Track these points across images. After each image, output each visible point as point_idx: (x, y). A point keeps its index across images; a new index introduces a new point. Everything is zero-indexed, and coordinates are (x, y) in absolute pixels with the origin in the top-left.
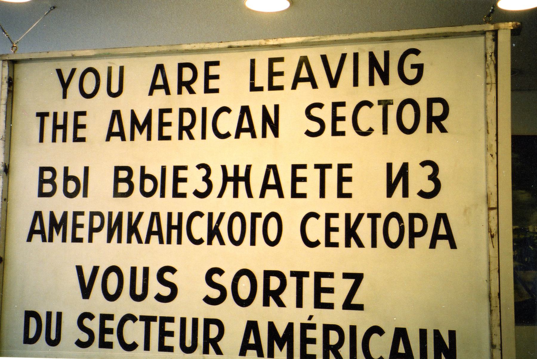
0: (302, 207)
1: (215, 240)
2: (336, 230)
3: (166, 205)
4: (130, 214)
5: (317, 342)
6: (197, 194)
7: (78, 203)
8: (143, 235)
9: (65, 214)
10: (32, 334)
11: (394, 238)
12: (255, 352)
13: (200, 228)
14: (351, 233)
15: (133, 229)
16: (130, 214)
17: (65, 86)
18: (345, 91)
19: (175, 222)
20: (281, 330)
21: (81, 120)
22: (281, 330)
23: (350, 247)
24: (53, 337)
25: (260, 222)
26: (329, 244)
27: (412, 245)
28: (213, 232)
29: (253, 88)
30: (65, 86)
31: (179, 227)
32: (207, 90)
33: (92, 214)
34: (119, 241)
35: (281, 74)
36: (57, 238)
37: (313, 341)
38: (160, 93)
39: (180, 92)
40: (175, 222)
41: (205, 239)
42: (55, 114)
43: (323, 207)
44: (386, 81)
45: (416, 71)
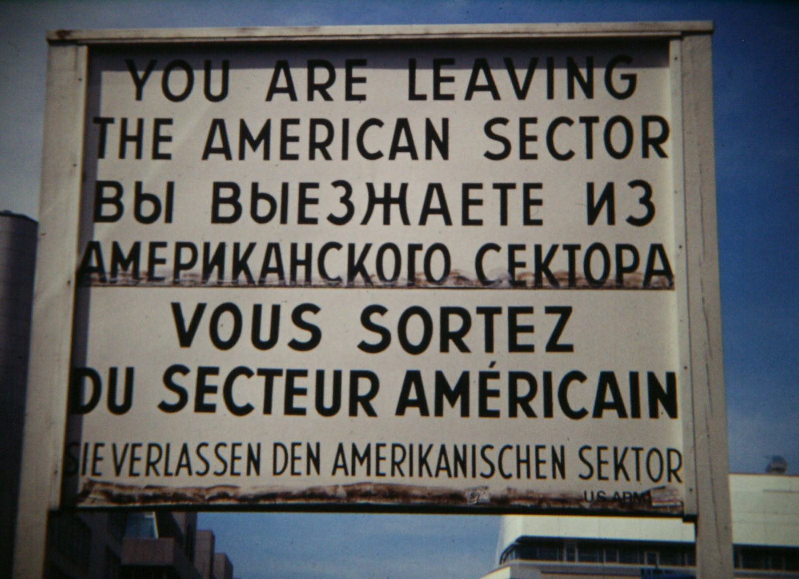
3: (288, 234)
4: (237, 246)
6: (332, 219)
7: (158, 230)
9: (136, 247)
15: (240, 265)
16: (237, 246)
20: (453, 384)
21: (164, 130)
22: (453, 384)
25: (420, 256)
28: (355, 268)
29: (413, 96)
32: (350, 97)
33: (179, 246)
37: (496, 394)
38: (281, 98)
39: (311, 97)
42: (124, 122)
43: (505, 237)
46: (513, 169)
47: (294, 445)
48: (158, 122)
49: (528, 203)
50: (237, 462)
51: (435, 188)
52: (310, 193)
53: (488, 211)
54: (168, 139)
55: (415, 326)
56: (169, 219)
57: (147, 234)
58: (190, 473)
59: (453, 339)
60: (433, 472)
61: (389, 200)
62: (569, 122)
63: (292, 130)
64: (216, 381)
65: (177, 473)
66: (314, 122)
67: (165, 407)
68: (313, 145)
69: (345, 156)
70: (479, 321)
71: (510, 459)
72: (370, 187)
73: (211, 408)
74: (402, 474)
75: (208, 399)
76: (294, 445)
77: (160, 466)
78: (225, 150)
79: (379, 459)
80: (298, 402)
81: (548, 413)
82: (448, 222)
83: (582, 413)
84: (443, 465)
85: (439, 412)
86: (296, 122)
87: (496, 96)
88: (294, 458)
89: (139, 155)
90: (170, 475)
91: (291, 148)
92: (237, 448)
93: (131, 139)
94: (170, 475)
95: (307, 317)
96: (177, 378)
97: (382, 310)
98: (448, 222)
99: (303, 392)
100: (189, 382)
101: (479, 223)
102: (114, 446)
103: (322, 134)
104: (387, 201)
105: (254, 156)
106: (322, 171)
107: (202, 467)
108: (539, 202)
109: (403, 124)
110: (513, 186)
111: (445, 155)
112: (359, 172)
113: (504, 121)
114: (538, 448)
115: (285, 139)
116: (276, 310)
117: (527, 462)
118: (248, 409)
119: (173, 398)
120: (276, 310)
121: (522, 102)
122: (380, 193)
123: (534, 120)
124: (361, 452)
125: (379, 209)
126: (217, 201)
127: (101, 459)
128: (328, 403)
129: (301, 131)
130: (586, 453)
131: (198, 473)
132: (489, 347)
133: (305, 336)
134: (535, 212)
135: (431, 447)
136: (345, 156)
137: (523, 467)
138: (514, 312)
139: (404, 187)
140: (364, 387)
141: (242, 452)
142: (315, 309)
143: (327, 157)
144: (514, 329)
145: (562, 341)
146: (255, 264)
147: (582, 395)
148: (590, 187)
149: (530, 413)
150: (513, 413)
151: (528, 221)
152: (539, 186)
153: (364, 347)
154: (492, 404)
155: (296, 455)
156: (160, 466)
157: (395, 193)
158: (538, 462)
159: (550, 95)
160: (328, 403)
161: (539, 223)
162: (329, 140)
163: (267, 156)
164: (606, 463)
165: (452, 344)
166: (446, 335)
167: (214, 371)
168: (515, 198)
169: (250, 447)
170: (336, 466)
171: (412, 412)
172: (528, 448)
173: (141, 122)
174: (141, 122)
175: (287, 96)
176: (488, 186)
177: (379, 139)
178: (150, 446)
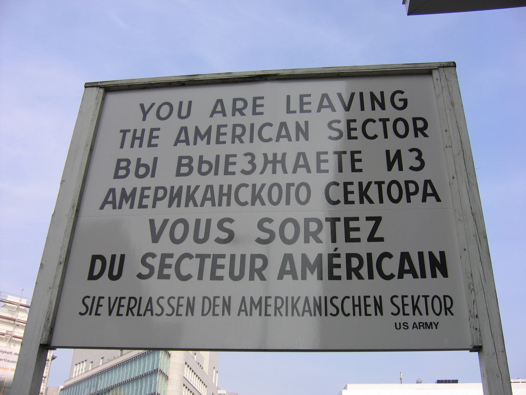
1: (258, 202)
2: (352, 192)
3: (217, 180)
4: (189, 187)
7: (147, 181)
9: (135, 190)
10: (96, 272)
11: (395, 196)
13: (245, 195)
14: (363, 194)
15: (190, 197)
16: (189, 187)
17: (145, 114)
19: (225, 191)
21: (155, 133)
22: (312, 259)
23: (363, 203)
24: (115, 273)
26: (347, 202)
27: (409, 201)
29: (289, 111)
30: (145, 114)
31: (229, 195)
32: (254, 113)
34: (179, 205)
36: (126, 206)
37: (339, 266)
39: (234, 115)
40: (225, 191)
41: (250, 201)
42: (135, 131)
44: (383, 107)
47: (215, 298)
48: (152, 130)
49: (353, 161)
50: (180, 308)
51: (301, 155)
52: (231, 160)
54: (157, 137)
56: (153, 176)
57: (140, 183)
58: (152, 315)
60: (301, 314)
61: (275, 162)
62: (374, 121)
63: (223, 130)
65: (144, 315)
66: (235, 126)
67: (140, 276)
68: (234, 136)
69: (251, 141)
70: (327, 226)
72: (265, 155)
73: (168, 277)
74: (281, 315)
75: (166, 271)
76: (215, 298)
77: (135, 311)
79: (267, 305)
80: (219, 272)
81: (371, 277)
82: (309, 171)
83: (392, 276)
84: (307, 309)
85: (304, 277)
87: (334, 110)
88: (215, 306)
89: (140, 146)
90: (141, 315)
91: (222, 138)
92: (181, 300)
93: (138, 138)
94: (141, 315)
95: (227, 225)
96: (149, 260)
97: (270, 221)
98: (309, 171)
99: (222, 267)
100: (155, 263)
102: (109, 298)
104: (274, 162)
106: (237, 148)
107: (159, 311)
108: (360, 160)
109: (283, 125)
111: (307, 139)
112: (259, 149)
114: (365, 297)
115: (219, 134)
116: (209, 222)
117: (359, 305)
118: (189, 277)
119: (145, 271)
120: (209, 222)
122: (270, 158)
123: (355, 121)
124: (256, 301)
125: (270, 166)
126: (180, 165)
127: (101, 306)
128: (237, 273)
129: (228, 130)
130: (395, 299)
131: (157, 315)
132: (334, 240)
133: (224, 236)
134: (358, 165)
135: (299, 298)
136: (251, 141)
137: (357, 309)
138: (347, 220)
139: (284, 155)
140: (259, 263)
141: (184, 302)
142: (231, 221)
143: (242, 142)
144: (348, 230)
145: (377, 235)
147: (391, 266)
148: (388, 152)
149: (360, 277)
150: (349, 277)
151: (354, 170)
152: (359, 152)
153: (260, 241)
154: (336, 272)
155: (216, 304)
156: (135, 311)
157: (279, 158)
158: (366, 306)
159: (362, 109)
160: (237, 273)
161: (361, 170)
163: (208, 143)
165: (311, 238)
167: (171, 256)
169: (188, 298)
170: (240, 310)
171: (288, 278)
172: (359, 297)
173: (143, 131)
174: (143, 131)
178: (130, 298)
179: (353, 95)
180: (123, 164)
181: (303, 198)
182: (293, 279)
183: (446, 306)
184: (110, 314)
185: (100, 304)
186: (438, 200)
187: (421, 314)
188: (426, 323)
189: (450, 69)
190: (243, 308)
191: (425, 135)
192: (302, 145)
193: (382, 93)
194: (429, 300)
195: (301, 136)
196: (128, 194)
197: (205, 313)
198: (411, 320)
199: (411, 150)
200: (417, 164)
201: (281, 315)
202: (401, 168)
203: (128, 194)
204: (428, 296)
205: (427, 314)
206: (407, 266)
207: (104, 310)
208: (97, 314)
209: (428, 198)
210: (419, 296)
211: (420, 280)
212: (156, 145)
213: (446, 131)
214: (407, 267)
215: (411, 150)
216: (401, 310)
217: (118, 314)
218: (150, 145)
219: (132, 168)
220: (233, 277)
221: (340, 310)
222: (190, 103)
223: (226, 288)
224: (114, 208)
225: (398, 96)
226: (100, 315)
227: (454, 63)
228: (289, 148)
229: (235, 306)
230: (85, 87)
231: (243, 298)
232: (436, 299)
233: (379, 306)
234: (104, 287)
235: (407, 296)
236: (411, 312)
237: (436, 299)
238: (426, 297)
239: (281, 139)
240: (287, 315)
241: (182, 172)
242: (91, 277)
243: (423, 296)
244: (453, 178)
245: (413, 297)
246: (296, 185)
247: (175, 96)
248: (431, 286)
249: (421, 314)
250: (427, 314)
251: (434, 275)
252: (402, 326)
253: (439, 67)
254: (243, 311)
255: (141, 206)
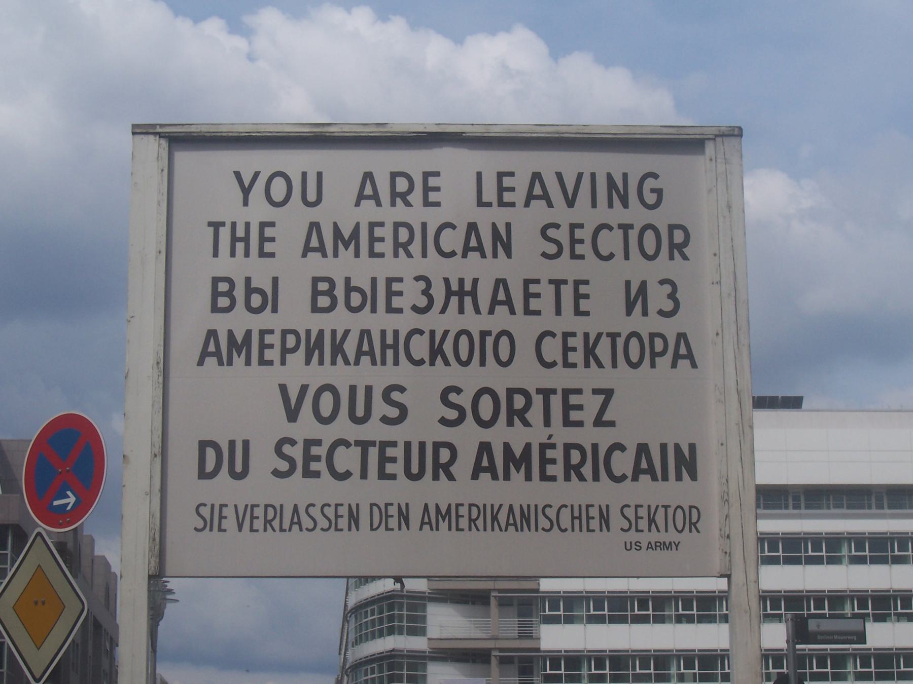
0: (537, 325)
2: (574, 349)
4: (334, 332)
5: (558, 462)
8: (351, 353)
9: (249, 333)
10: (210, 466)
11: (634, 358)
12: (489, 475)
13: (420, 347)
14: (590, 352)
15: (338, 349)
16: (334, 332)
17: (246, 191)
18: (583, 212)
19: (390, 340)
20: (518, 451)
21: (269, 232)
22: (518, 451)
24: (239, 468)
26: (567, 364)
27: (653, 365)
29: (481, 203)
30: (246, 191)
31: (395, 347)
32: (427, 203)
33: (285, 333)
34: (321, 362)
35: (512, 189)
36: (239, 361)
37: (553, 461)
38: (368, 205)
39: (393, 204)
40: (390, 340)
41: (427, 359)
42: (234, 225)
43: (559, 325)
45: (655, 196)
46: (565, 268)
47: (387, 505)
49: (578, 297)
50: (339, 519)
51: (501, 283)
52: (396, 287)
53: (544, 304)
54: (272, 240)
55: (486, 403)
56: (275, 310)
57: (257, 323)
58: (301, 530)
59: (517, 416)
60: (503, 526)
62: (610, 228)
63: (378, 232)
64: (320, 451)
65: (290, 530)
66: (397, 225)
67: (276, 473)
68: (397, 245)
69: (424, 255)
70: (538, 400)
71: (566, 516)
72: (447, 281)
73: (317, 474)
74: (478, 530)
75: (314, 466)
76: (387, 505)
77: (276, 524)
78: (322, 250)
79: (458, 516)
80: (390, 468)
81: (596, 478)
82: (512, 312)
83: (623, 478)
84: (511, 521)
85: (507, 477)
86: (381, 224)
87: (550, 205)
88: (387, 516)
89: (247, 254)
90: (285, 531)
93: (240, 240)
94: (285, 531)
95: (396, 396)
96: (287, 449)
97: (458, 391)
98: (512, 312)
99: (394, 460)
100: (296, 452)
101: (538, 313)
102: (236, 506)
103: (404, 235)
104: (461, 293)
105: (346, 254)
106: (405, 267)
107: (311, 526)
108: (586, 296)
109: (472, 228)
110: (565, 282)
111: (509, 255)
112: (436, 268)
113: (557, 226)
114: (588, 506)
115: (373, 240)
116: (369, 390)
117: (580, 518)
118: (347, 475)
119: (284, 466)
120: (369, 390)
121: (571, 209)
122: (455, 287)
123: (581, 226)
125: (454, 300)
126: (316, 293)
127: (226, 517)
128: (415, 469)
129: (385, 232)
130: (626, 510)
131: (307, 529)
132: (547, 423)
133: (394, 413)
134: (584, 305)
135: (501, 506)
136: (424, 255)
137: (577, 522)
138: (567, 393)
139: (475, 281)
141: (344, 511)
142: (402, 389)
143: (409, 255)
144: (567, 408)
145: (606, 417)
146: (350, 347)
147: (623, 463)
148: (628, 284)
149: (581, 478)
150: (567, 478)
151: (578, 312)
152: (586, 282)
153: (444, 421)
154: (550, 470)
155: (389, 513)
156: (276, 524)
157: (468, 287)
158: (589, 518)
159: (594, 205)
160: (415, 469)
161: (587, 314)
162: (411, 240)
163: (357, 255)
164: (642, 518)
165: (516, 420)
166: (512, 413)
167: (318, 443)
168: (567, 292)
169: (350, 505)
170: (423, 523)
171: (485, 477)
172: (580, 506)
173: (248, 225)
174: (248, 225)
175: (373, 202)
176: (544, 282)
177: (452, 240)
178: (266, 506)
179: (580, 175)
180: (223, 287)
181: (504, 355)
182: (493, 479)
183: (691, 519)
184: (240, 527)
185: (223, 515)
186: (694, 365)
187: (659, 531)
188: (664, 543)
189: (733, 139)
190: (426, 520)
191: (685, 258)
192: (500, 267)
193: (625, 176)
194: (670, 512)
195: (500, 249)
196: (239, 340)
197: (375, 526)
198: (645, 538)
199: (662, 282)
200: (668, 306)
201: (478, 530)
202: (645, 313)
203: (239, 340)
204: (669, 506)
205: (666, 531)
206: (645, 464)
207: (230, 523)
208: (220, 530)
209: (680, 362)
210: (657, 507)
211: (660, 484)
212: (272, 255)
213: (715, 255)
214: (644, 465)
215: (662, 282)
216: (632, 525)
217: (252, 530)
218: (262, 254)
219: (239, 293)
220: (409, 475)
221: (555, 524)
222: (320, 175)
223: (400, 491)
224: (221, 363)
225: (650, 183)
226: (225, 531)
227: (740, 129)
228: (483, 270)
229: (415, 516)
230: (133, 133)
231: (426, 505)
232: (679, 511)
233: (605, 519)
234: (223, 490)
235: (641, 506)
236: (646, 528)
237: (679, 511)
238: (666, 507)
239: (469, 253)
240: (485, 530)
241: (319, 305)
242: (203, 474)
243: (663, 506)
244: (717, 334)
245: (649, 506)
246: (494, 334)
247: (295, 162)
248: (674, 492)
249: (659, 531)
250: (666, 531)
251: (679, 478)
252: (634, 546)
253: (716, 136)
254: (426, 523)
255: (262, 362)
